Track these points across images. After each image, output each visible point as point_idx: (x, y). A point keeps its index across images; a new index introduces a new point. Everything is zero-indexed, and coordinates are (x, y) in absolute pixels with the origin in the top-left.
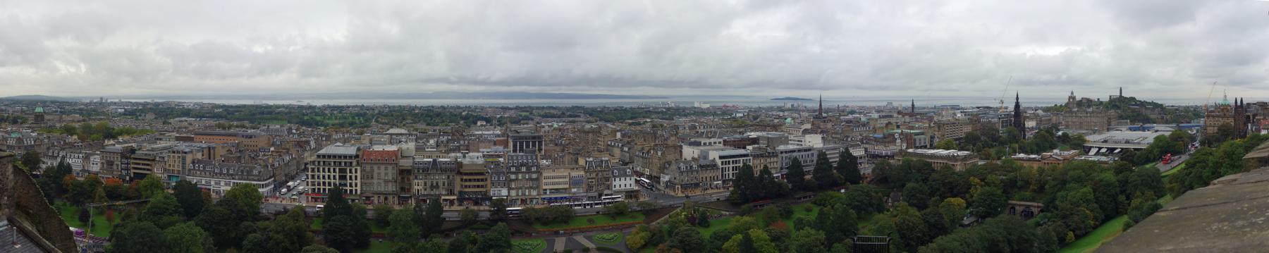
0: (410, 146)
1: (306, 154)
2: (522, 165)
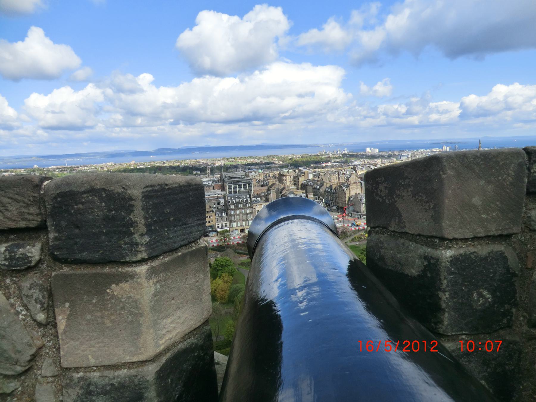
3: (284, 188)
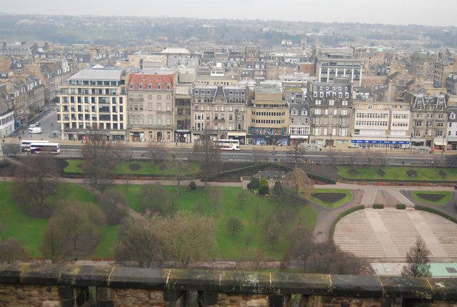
0: (188, 70)
1: (58, 80)
2: (330, 97)
3: (412, 82)
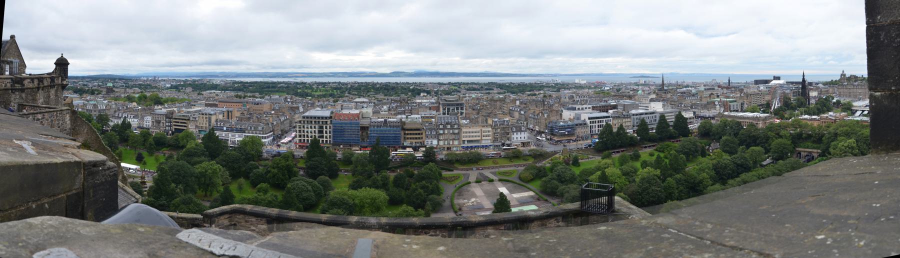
2: (447, 124)
